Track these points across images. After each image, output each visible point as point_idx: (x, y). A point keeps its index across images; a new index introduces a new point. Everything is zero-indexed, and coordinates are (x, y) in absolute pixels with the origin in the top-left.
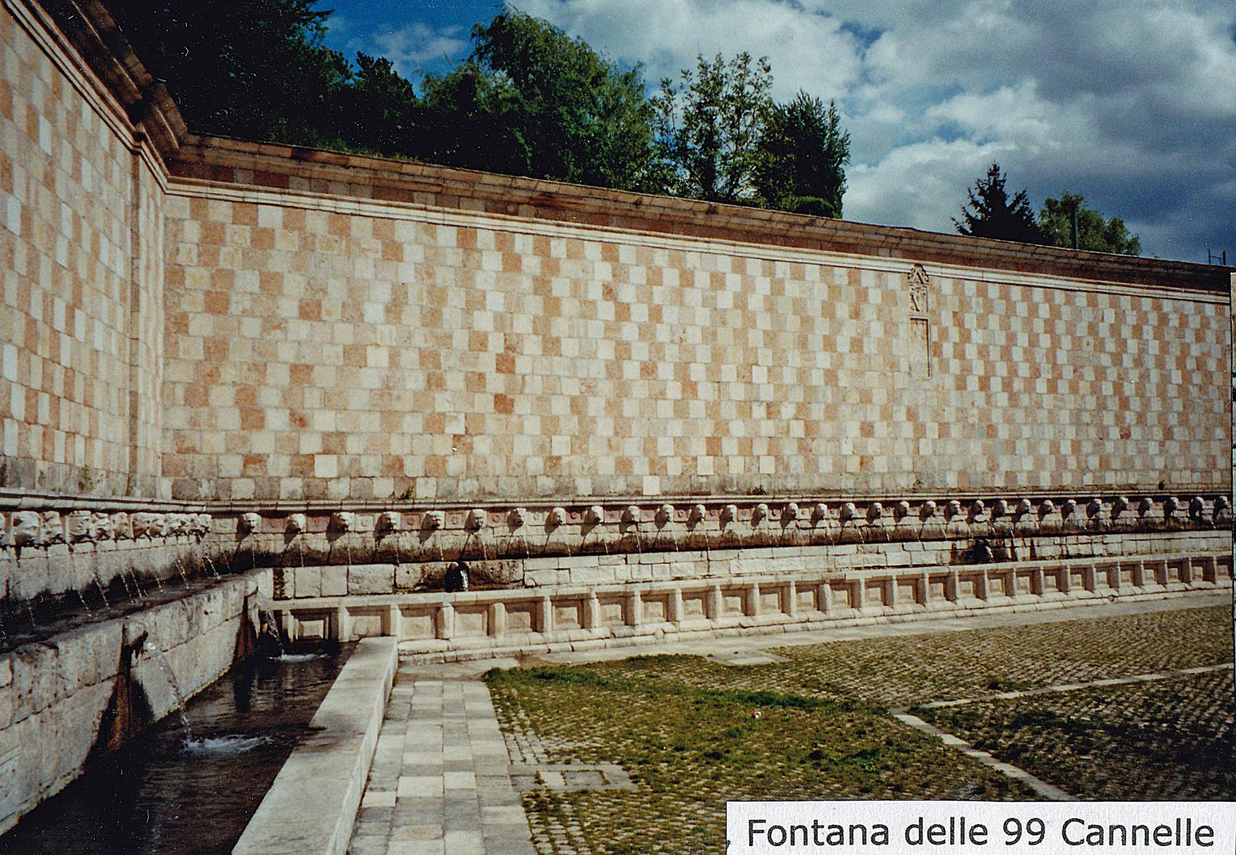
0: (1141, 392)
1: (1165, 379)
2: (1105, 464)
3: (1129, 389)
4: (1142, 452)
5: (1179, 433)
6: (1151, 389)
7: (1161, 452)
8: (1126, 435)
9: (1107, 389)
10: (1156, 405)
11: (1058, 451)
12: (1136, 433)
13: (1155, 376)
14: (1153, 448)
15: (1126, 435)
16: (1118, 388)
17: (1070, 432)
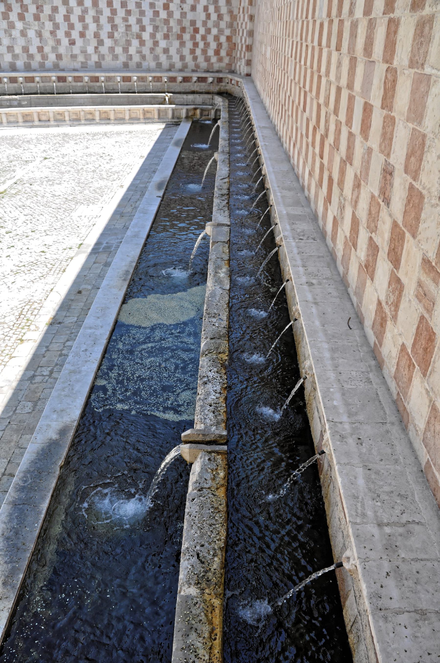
0: (82, 19)
1: (99, 12)
2: (59, 57)
3: (74, 19)
4: (84, 52)
5: (108, 43)
6: (89, 19)
7: (96, 52)
8: (72, 43)
9: (59, 18)
10: (93, 27)
11: (28, 51)
12: (79, 42)
13: (92, 13)
14: (90, 50)
15: (72, 43)
16: (67, 18)
17: (36, 42)
